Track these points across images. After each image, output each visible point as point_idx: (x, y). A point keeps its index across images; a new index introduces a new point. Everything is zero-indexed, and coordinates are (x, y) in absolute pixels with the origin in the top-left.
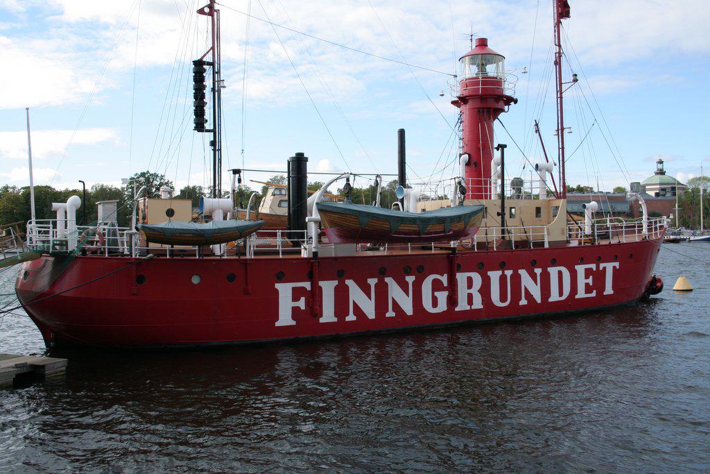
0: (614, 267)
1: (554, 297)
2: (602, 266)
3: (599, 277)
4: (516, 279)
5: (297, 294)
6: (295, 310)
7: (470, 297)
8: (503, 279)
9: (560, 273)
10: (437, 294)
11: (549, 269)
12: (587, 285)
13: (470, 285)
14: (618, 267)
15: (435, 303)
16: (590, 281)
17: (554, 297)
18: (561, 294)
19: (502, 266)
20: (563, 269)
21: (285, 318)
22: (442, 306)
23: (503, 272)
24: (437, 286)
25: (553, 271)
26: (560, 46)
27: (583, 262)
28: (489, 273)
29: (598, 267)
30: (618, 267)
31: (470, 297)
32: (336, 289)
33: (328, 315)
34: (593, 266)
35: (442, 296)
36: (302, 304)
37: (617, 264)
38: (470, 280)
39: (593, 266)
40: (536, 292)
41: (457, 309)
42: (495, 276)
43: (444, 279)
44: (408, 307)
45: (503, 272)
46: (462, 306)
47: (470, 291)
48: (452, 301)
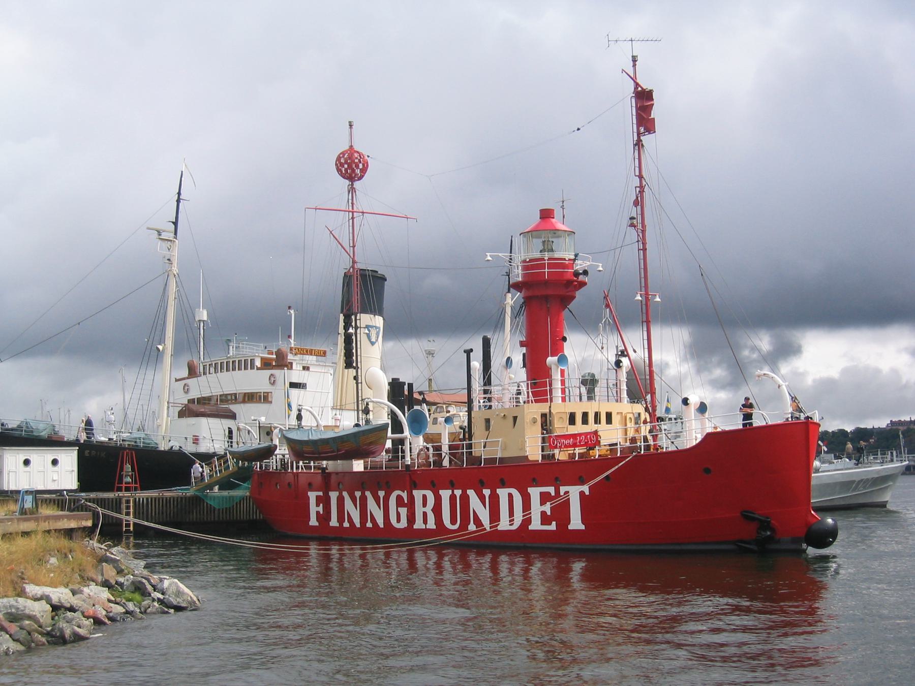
0: (582, 493)
1: (504, 524)
2: (563, 489)
4: (465, 499)
6: (318, 513)
7: (425, 514)
8: (453, 498)
9: (510, 496)
10: (399, 509)
11: (499, 491)
12: (543, 514)
14: (587, 493)
16: (547, 508)
19: (453, 487)
20: (514, 492)
21: (313, 522)
22: (403, 524)
23: (453, 492)
24: (400, 502)
25: (503, 493)
26: (641, 177)
28: (441, 492)
29: (557, 491)
30: (587, 493)
31: (425, 514)
32: (338, 498)
33: (334, 522)
34: (551, 490)
35: (403, 511)
38: (425, 497)
39: (551, 490)
40: (484, 515)
41: (415, 527)
42: (445, 494)
43: (405, 495)
44: (380, 522)
45: (453, 492)
46: (419, 524)
47: (424, 509)
48: (411, 519)
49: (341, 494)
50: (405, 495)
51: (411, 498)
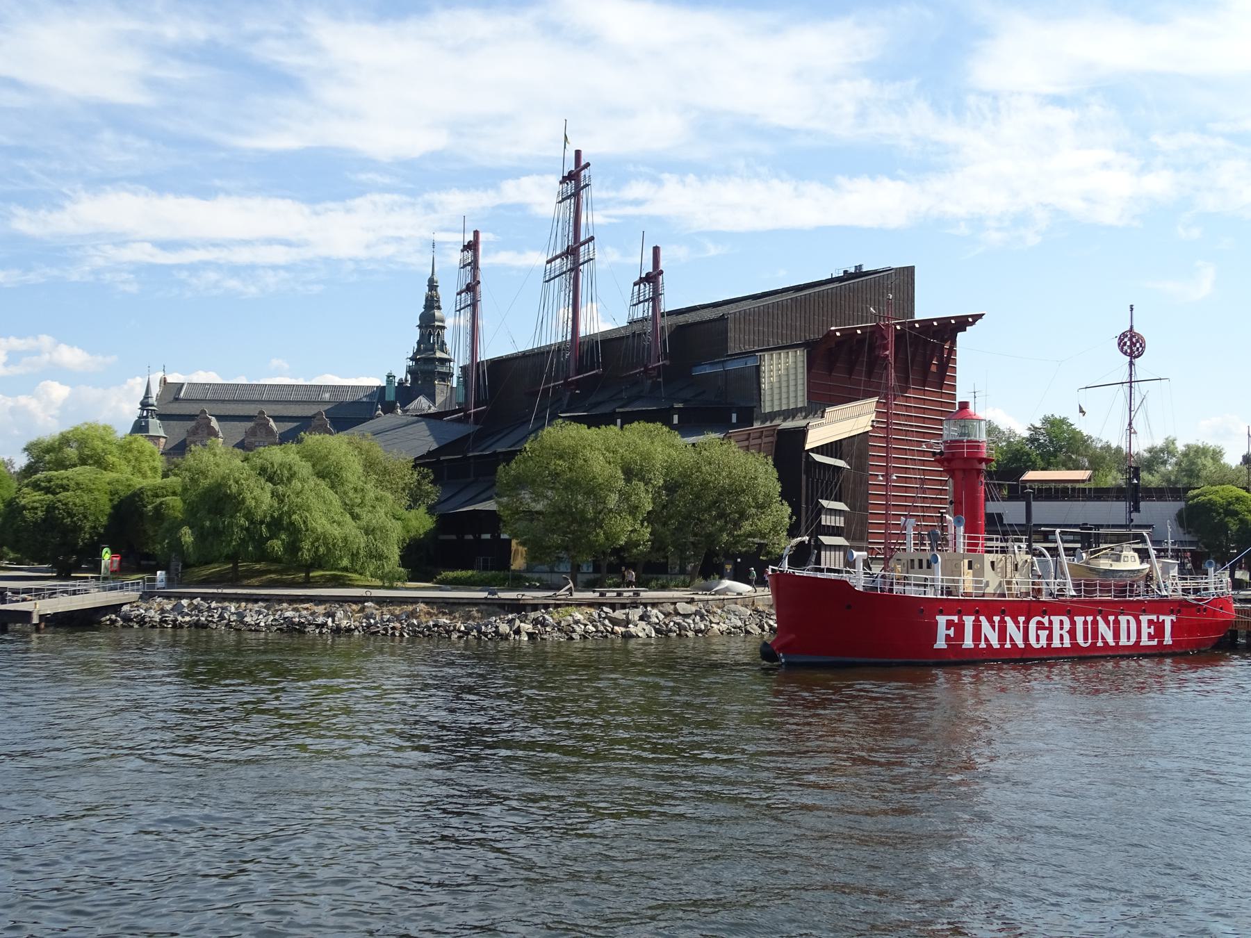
1: (1123, 641)
2: (1161, 618)
3: (1159, 628)
5: (949, 624)
6: (948, 636)
7: (1061, 636)
8: (1085, 622)
9: (1128, 621)
13: (1062, 628)
15: (1038, 640)
16: (1152, 630)
17: (1123, 641)
18: (1129, 638)
21: (941, 644)
22: (1043, 642)
24: (1040, 626)
27: (1145, 612)
31: (1061, 636)
33: (968, 642)
34: (1154, 617)
35: (1044, 634)
36: (951, 632)
37: (1174, 618)
38: (1062, 622)
39: (1154, 617)
42: (1079, 620)
46: (1056, 643)
48: (1050, 638)
49: (977, 621)
50: (1045, 620)
51: (1051, 622)
